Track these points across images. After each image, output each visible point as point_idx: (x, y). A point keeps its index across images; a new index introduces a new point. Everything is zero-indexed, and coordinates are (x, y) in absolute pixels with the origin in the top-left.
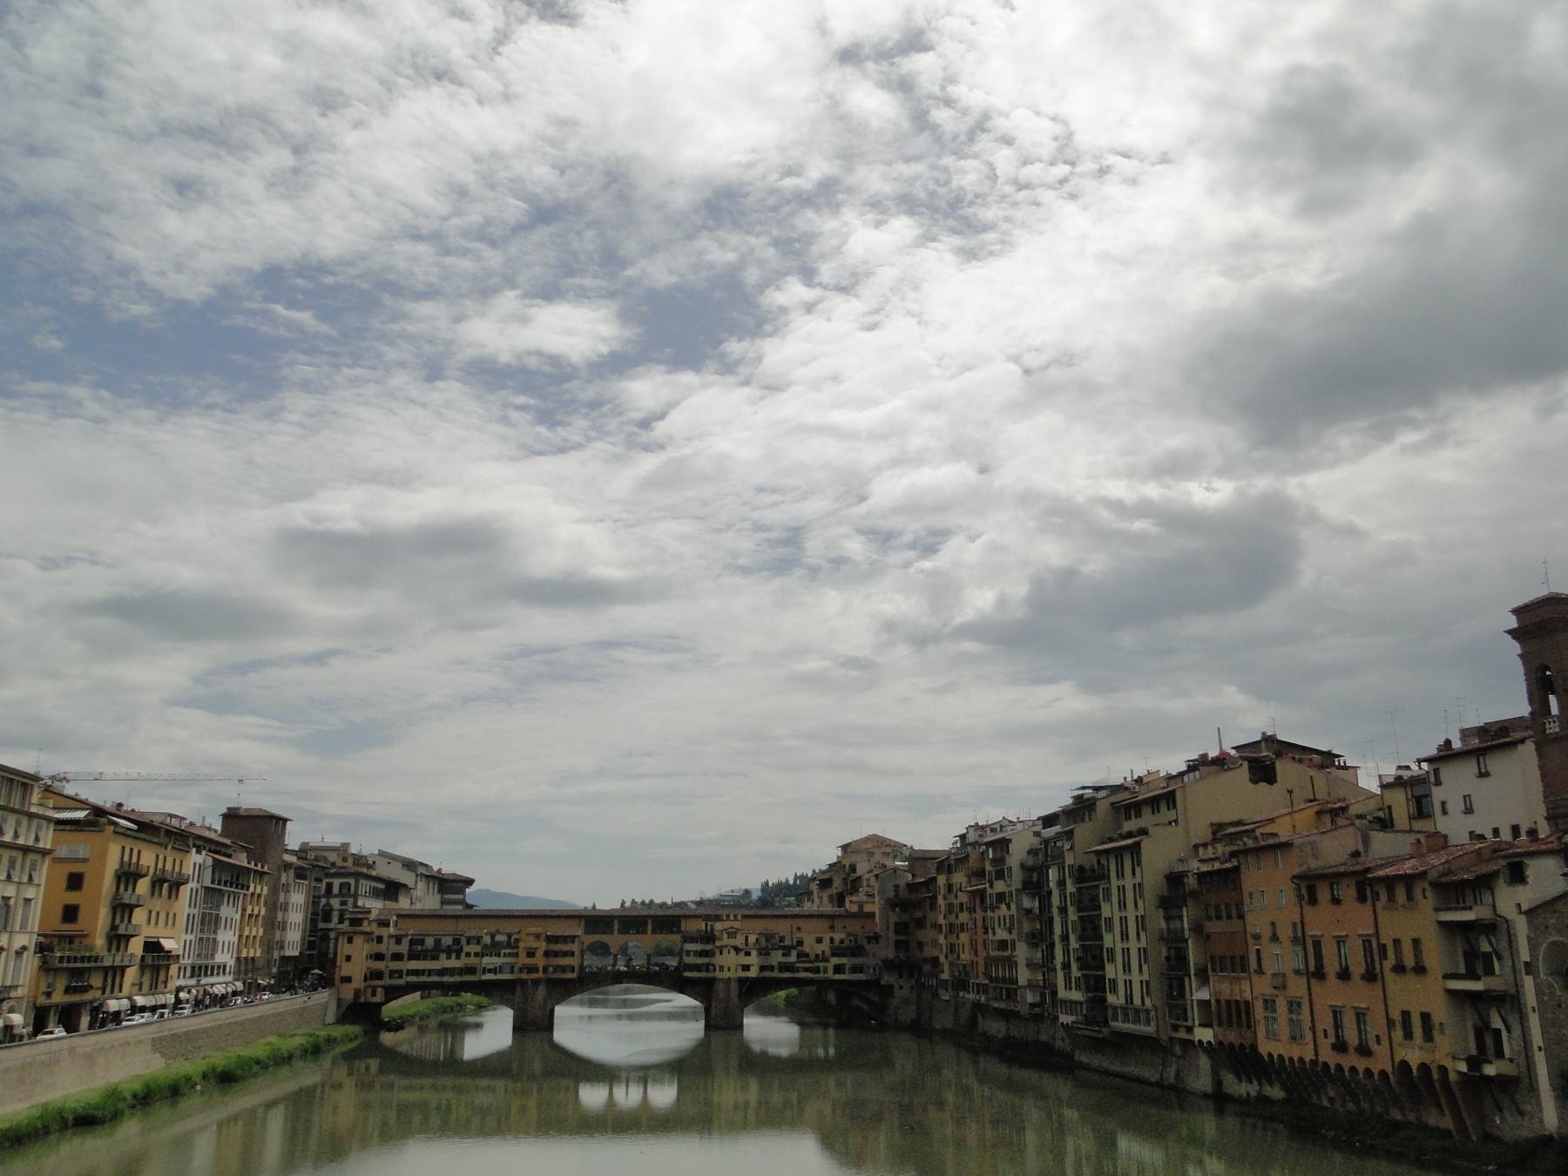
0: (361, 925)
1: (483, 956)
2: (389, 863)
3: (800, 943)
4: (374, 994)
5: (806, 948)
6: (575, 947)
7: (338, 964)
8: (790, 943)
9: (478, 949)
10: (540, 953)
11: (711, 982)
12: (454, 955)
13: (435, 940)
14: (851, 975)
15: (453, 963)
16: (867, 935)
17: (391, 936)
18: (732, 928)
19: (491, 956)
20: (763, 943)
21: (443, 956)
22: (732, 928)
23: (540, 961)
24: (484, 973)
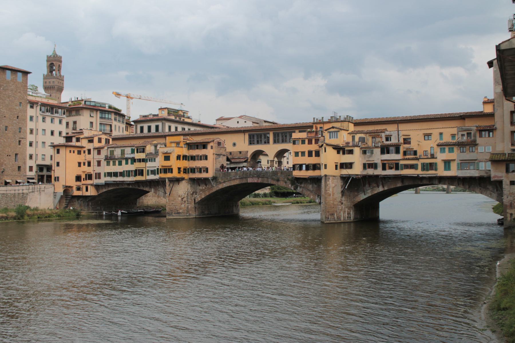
0: (71, 141)
1: (147, 161)
2: (245, 122)
3: (407, 141)
4: (87, 190)
5: (414, 145)
6: (209, 152)
7: (53, 169)
8: (397, 142)
9: (142, 156)
10: (173, 157)
11: (317, 181)
12: (129, 161)
13: (122, 150)
14: (460, 171)
15: (131, 167)
16: (479, 129)
17: (95, 149)
18: (333, 127)
19: (152, 161)
20: (370, 141)
21: (124, 162)
22: (333, 127)
23: (174, 163)
24: (148, 174)
